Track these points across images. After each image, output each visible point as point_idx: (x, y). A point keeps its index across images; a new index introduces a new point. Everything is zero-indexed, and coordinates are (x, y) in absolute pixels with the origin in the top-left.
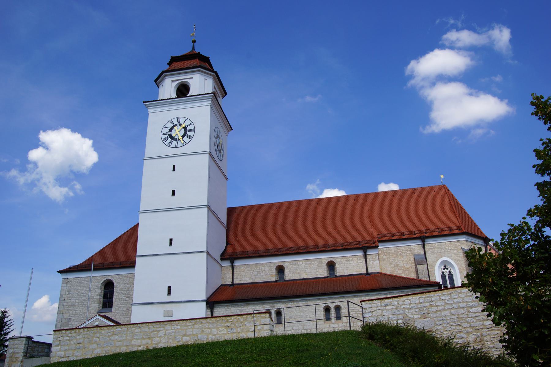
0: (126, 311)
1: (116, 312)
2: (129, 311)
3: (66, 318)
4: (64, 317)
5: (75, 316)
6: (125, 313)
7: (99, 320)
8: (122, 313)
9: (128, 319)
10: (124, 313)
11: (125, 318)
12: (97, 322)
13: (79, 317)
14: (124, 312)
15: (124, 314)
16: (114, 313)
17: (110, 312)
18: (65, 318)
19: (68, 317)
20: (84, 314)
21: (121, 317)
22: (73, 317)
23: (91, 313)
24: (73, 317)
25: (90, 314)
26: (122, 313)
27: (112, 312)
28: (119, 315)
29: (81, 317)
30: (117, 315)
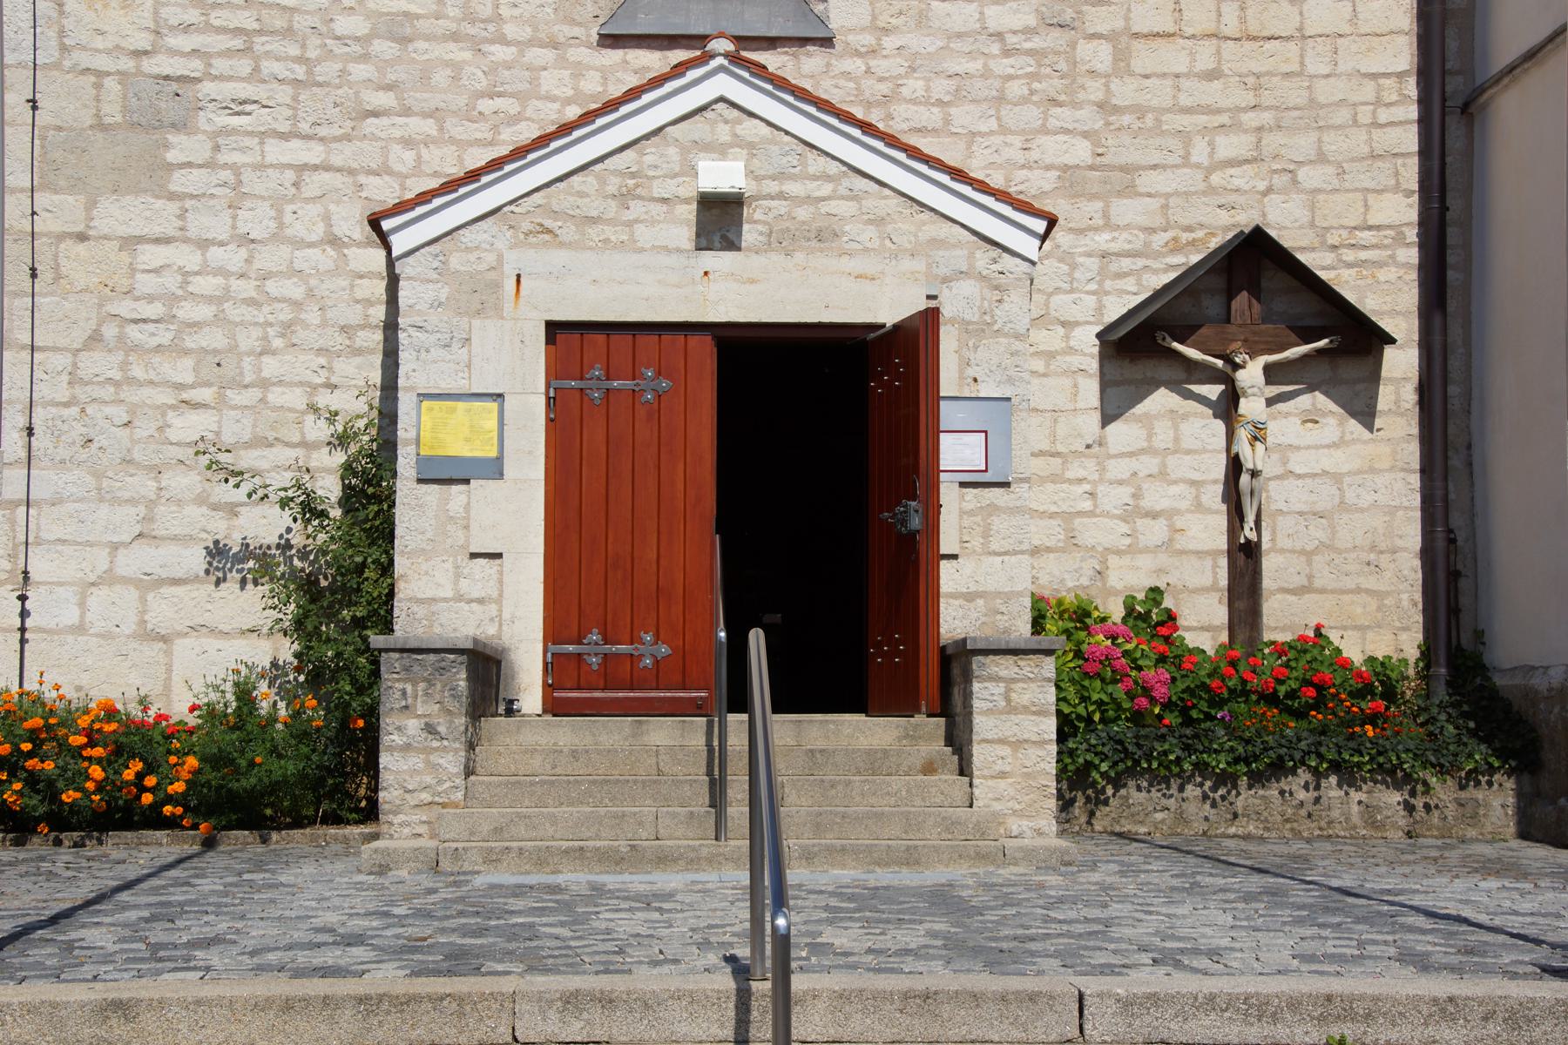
0: (1036, 43)
1: (890, 43)
2: (1085, 49)
3: (103, 63)
4: (64, 48)
5: (247, 50)
6: (1027, 65)
7: (750, 128)
8: (975, 66)
9: (1069, 159)
10: (1003, 66)
11: (1029, 137)
12: (720, 151)
13: (328, 70)
14: (1007, 53)
15: (1016, 89)
16: (856, 65)
17: (804, 41)
18: (85, 60)
19: (138, 54)
20: (405, 41)
21: (963, 116)
22: (220, 66)
23: (510, 30)
24: (220, 66)
25: (500, 53)
26: (975, 66)
27: (827, 42)
28: (941, 88)
29: (360, 71)
30: (914, 86)
